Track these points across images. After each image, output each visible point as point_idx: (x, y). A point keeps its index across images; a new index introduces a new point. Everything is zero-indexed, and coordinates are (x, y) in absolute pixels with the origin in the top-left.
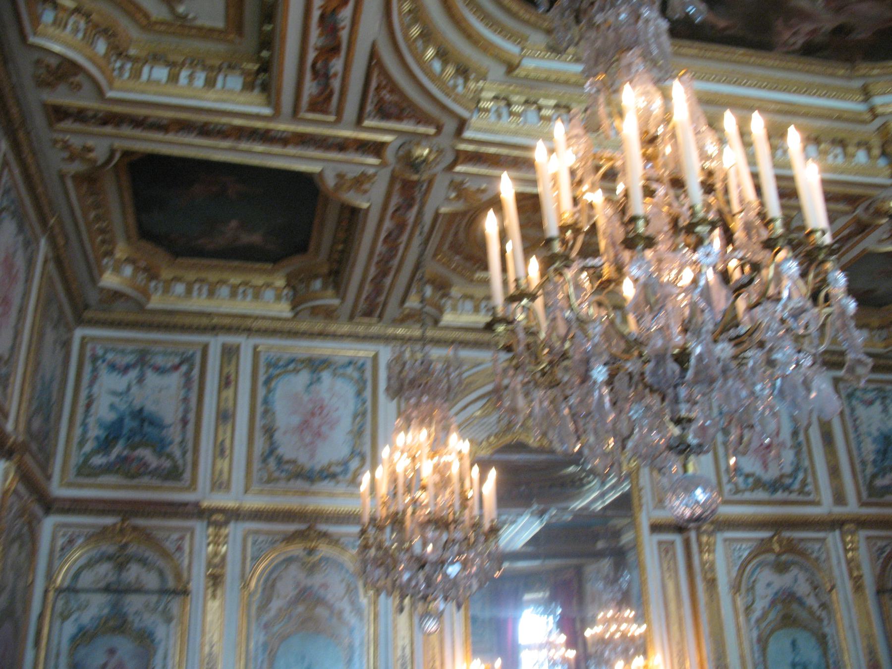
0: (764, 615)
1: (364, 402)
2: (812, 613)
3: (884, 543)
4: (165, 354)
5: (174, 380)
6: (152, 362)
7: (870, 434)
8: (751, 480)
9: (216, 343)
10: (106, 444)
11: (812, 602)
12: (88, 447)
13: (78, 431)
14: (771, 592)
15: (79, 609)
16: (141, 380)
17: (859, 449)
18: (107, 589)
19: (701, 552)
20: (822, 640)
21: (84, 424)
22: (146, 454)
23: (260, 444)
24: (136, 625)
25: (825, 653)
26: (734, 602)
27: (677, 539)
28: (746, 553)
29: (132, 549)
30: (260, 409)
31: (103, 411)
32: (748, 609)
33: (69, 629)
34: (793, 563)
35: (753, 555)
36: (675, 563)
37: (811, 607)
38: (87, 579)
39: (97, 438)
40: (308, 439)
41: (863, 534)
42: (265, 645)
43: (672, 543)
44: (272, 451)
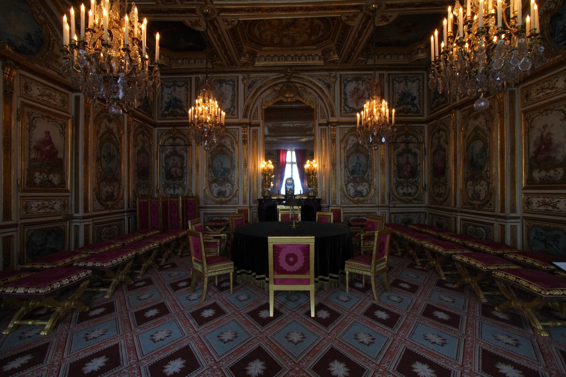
0: (350, 149)
1: (235, 91)
2: (365, 148)
5: (183, 89)
7: (398, 93)
8: (351, 109)
10: (167, 109)
12: (163, 110)
13: (160, 105)
16: (174, 90)
17: (393, 98)
18: (172, 145)
20: (367, 157)
21: (162, 103)
22: (178, 110)
25: (367, 161)
26: (340, 145)
27: (326, 127)
29: (177, 135)
31: (166, 99)
32: (345, 148)
33: (164, 155)
35: (349, 131)
38: (167, 143)
39: (165, 107)
42: (211, 157)
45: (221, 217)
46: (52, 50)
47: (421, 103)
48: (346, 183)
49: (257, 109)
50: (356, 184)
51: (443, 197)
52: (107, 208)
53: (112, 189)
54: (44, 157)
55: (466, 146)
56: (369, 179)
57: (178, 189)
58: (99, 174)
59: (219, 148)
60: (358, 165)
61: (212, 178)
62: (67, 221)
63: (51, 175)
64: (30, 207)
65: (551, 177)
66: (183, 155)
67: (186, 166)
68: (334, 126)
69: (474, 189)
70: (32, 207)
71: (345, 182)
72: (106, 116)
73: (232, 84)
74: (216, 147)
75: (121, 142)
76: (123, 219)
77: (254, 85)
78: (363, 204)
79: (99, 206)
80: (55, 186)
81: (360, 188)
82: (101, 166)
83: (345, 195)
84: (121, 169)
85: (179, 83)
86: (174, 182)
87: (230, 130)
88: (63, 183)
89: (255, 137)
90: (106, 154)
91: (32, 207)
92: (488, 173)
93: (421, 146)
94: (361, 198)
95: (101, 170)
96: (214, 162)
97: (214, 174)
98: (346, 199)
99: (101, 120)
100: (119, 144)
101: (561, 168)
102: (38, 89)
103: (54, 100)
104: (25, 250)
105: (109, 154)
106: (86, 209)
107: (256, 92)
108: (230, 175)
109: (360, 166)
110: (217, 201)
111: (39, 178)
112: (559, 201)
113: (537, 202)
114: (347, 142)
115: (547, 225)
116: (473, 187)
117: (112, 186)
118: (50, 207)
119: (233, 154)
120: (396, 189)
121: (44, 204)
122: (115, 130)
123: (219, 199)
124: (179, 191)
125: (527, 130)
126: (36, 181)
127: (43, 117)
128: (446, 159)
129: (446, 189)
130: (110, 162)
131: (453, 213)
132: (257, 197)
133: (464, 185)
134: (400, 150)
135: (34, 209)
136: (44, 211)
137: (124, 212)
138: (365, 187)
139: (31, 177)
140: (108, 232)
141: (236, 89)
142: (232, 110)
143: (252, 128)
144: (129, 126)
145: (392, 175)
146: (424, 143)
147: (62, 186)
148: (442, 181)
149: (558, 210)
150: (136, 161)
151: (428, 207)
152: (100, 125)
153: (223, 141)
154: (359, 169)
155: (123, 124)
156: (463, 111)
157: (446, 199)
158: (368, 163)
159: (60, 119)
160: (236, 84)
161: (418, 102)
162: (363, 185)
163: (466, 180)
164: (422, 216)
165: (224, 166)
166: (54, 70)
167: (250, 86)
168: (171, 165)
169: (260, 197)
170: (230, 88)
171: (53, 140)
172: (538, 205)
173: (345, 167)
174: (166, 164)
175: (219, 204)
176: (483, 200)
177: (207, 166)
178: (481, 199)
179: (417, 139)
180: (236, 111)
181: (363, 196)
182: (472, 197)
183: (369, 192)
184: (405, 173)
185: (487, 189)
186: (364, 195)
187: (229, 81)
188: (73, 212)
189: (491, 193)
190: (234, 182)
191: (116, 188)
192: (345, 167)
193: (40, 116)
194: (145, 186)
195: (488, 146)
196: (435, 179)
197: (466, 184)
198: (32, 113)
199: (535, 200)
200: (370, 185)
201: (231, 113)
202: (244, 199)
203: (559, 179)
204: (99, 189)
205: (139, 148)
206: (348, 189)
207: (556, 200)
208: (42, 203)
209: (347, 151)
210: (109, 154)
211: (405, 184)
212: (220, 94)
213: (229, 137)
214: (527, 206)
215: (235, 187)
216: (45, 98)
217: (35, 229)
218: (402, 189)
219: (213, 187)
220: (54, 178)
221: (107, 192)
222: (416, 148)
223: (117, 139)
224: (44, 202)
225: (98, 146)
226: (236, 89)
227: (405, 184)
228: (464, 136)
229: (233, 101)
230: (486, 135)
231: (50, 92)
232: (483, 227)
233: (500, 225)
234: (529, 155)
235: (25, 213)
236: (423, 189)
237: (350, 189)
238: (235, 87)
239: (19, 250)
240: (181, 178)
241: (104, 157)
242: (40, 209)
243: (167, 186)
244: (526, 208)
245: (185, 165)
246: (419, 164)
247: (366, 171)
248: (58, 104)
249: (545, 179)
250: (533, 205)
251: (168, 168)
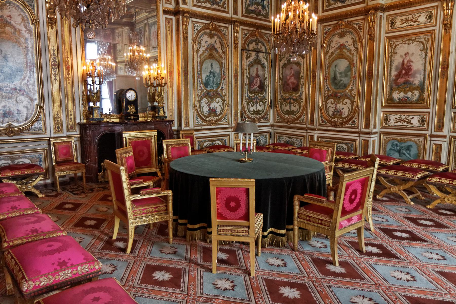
0: (203, 53)
2: (219, 55)
3: (247, 32)
11: (220, 51)
14: (206, 45)
19: (183, 24)
20: (221, 65)
25: (221, 70)
27: (173, 18)
28: (199, 28)
34: (216, 35)
35: (202, 29)
36: (172, 28)
37: (219, 52)
41: (241, 27)
43: (171, 19)
45: (13, 159)
47: (269, 6)
48: (200, 97)
50: (210, 99)
51: (295, 115)
55: (327, 63)
56: (222, 93)
60: (212, 75)
65: (408, 98)
68: (187, 18)
69: (335, 107)
71: (198, 96)
78: (216, 125)
81: (214, 105)
83: (199, 114)
92: (353, 92)
93: (268, 57)
94: (215, 118)
98: (199, 119)
101: (417, 91)
109: (214, 76)
112: (413, 118)
113: (395, 119)
114: (200, 44)
115: (402, 138)
116: (334, 105)
120: (248, 105)
125: (390, 55)
128: (301, 74)
129: (300, 106)
131: (309, 131)
132: (75, 119)
133: (324, 103)
134: (251, 59)
138: (219, 104)
145: (244, 90)
146: (271, 54)
148: (294, 98)
149: (412, 125)
151: (273, 126)
154: (213, 81)
156: (326, 26)
157: (300, 116)
158: (221, 73)
161: (267, 4)
162: (217, 101)
163: (327, 98)
164: (268, 136)
172: (395, 121)
173: (198, 77)
176: (346, 117)
178: (344, 116)
179: (266, 48)
181: (216, 116)
182: (333, 114)
183: (223, 109)
184: (255, 87)
185: (350, 108)
186: (218, 113)
189: (354, 112)
192: (199, 76)
195: (354, 66)
196: (284, 95)
197: (326, 102)
199: (392, 118)
200: (224, 101)
202: (55, 124)
203: (414, 100)
206: (202, 106)
207: (411, 117)
209: (200, 55)
211: (255, 101)
214: (385, 123)
218: (252, 106)
222: (265, 58)
227: (255, 101)
228: (327, 53)
230: (353, 54)
232: (344, 143)
233: (364, 140)
234: (390, 78)
236: (269, 105)
237: (203, 107)
244: (384, 124)
246: (266, 78)
247: (220, 84)
249: (403, 99)
250: (391, 121)
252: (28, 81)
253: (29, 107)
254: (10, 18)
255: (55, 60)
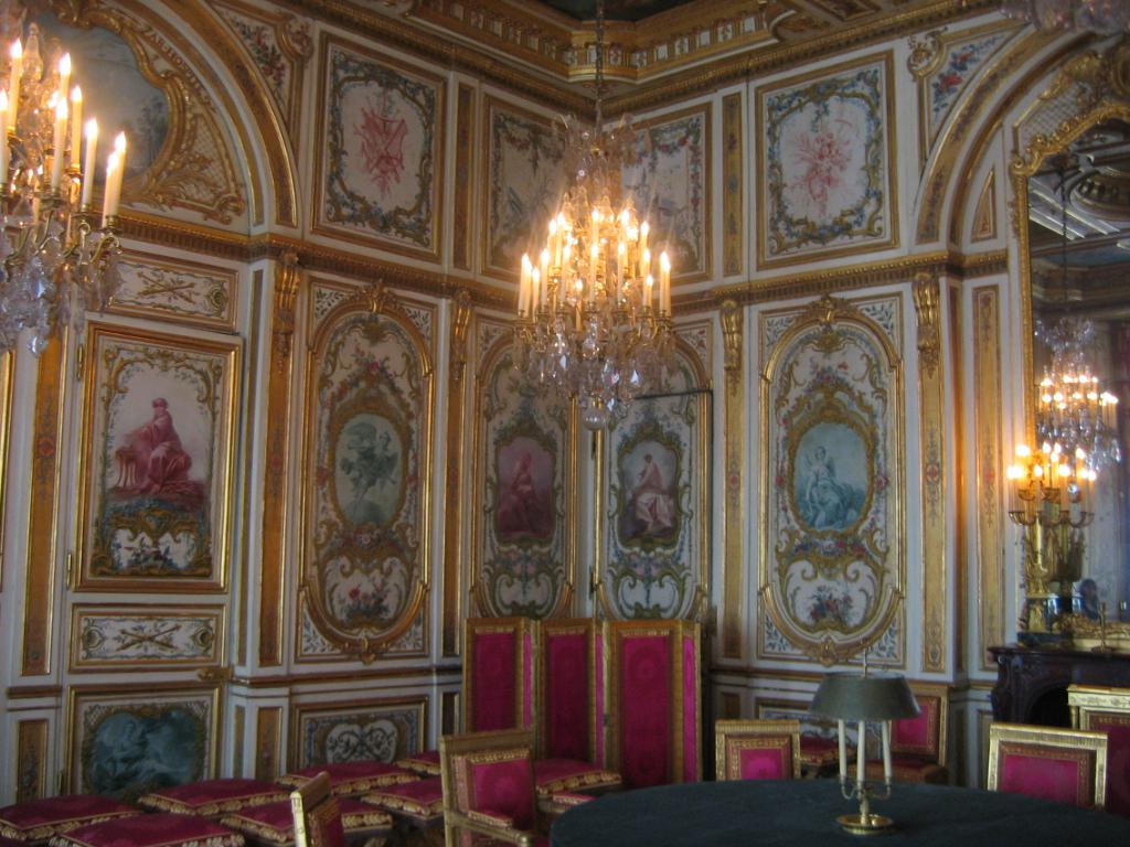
1: (878, 124)
4: (673, 129)
5: (684, 153)
6: (661, 143)
9: (716, 98)
15: (623, 418)
16: (653, 166)
23: (769, 208)
24: (666, 429)
30: (767, 164)
33: (616, 439)
40: (817, 190)
42: (786, 439)
44: (781, 213)
46: (189, 148)
49: (992, 185)
52: (353, 651)
53: (378, 581)
54: (147, 481)
57: (661, 586)
58: (324, 529)
59: (820, 396)
61: (792, 534)
62: (214, 688)
63: (167, 538)
64: (98, 639)
66: (678, 437)
67: (687, 485)
70: (104, 639)
72: (363, 321)
73: (867, 91)
74: (809, 391)
75: (421, 404)
76: (422, 699)
77: (965, 76)
79: (319, 644)
80: (177, 573)
82: (334, 499)
84: (418, 508)
85: (667, 136)
86: (648, 552)
87: (862, 306)
88: (203, 563)
89: (987, 327)
90: (354, 456)
91: (104, 639)
95: (333, 515)
96: (800, 461)
97: (798, 517)
99: (340, 338)
100: (410, 416)
102: (140, 275)
103: (188, 300)
104: (80, 767)
105: (368, 455)
106: (267, 655)
107: (973, 108)
108: (869, 521)
110: (811, 646)
111: (130, 549)
117: (376, 572)
118: (158, 639)
119: (878, 420)
121: (142, 628)
122: (396, 365)
123: (818, 637)
124: (663, 595)
126: (119, 556)
127: (149, 359)
130: (372, 483)
135: (111, 645)
136: (141, 651)
137: (426, 671)
139: (104, 542)
140: (354, 740)
141: (882, 113)
142: (869, 210)
143: (969, 285)
144: (456, 343)
147: (201, 571)
150: (491, 472)
152: (335, 354)
153: (835, 360)
155: (434, 338)
159: (202, 357)
160: (882, 87)
165: (840, 479)
166: (193, 208)
167: (947, 83)
168: (637, 483)
169: (1011, 639)
170: (855, 112)
171: (175, 424)
174: (622, 475)
175: (818, 662)
177: (773, 480)
180: (886, 211)
187: (853, 85)
188: (235, 660)
190: (884, 556)
191: (396, 579)
193: (141, 356)
194: (531, 570)
198: (119, 349)
201: (865, 225)
204: (323, 582)
205: (505, 419)
208: (135, 625)
210: (368, 455)
212: (818, 146)
213: (861, 338)
215: (887, 578)
216: (161, 299)
217: (110, 708)
219: (795, 581)
220: (174, 547)
221: (354, 593)
223: (405, 396)
224: (143, 624)
225: (324, 431)
226: (882, 113)
229: (872, 168)
231: (175, 277)
235: (83, 653)
238: (880, 103)
239: (62, 766)
240: (669, 535)
241: (348, 467)
242: (128, 646)
243: (624, 570)
245: (684, 477)
248: (200, 309)
251: (629, 495)
252: (873, 523)
253: (871, 594)
254: (843, 370)
255: (936, 458)
